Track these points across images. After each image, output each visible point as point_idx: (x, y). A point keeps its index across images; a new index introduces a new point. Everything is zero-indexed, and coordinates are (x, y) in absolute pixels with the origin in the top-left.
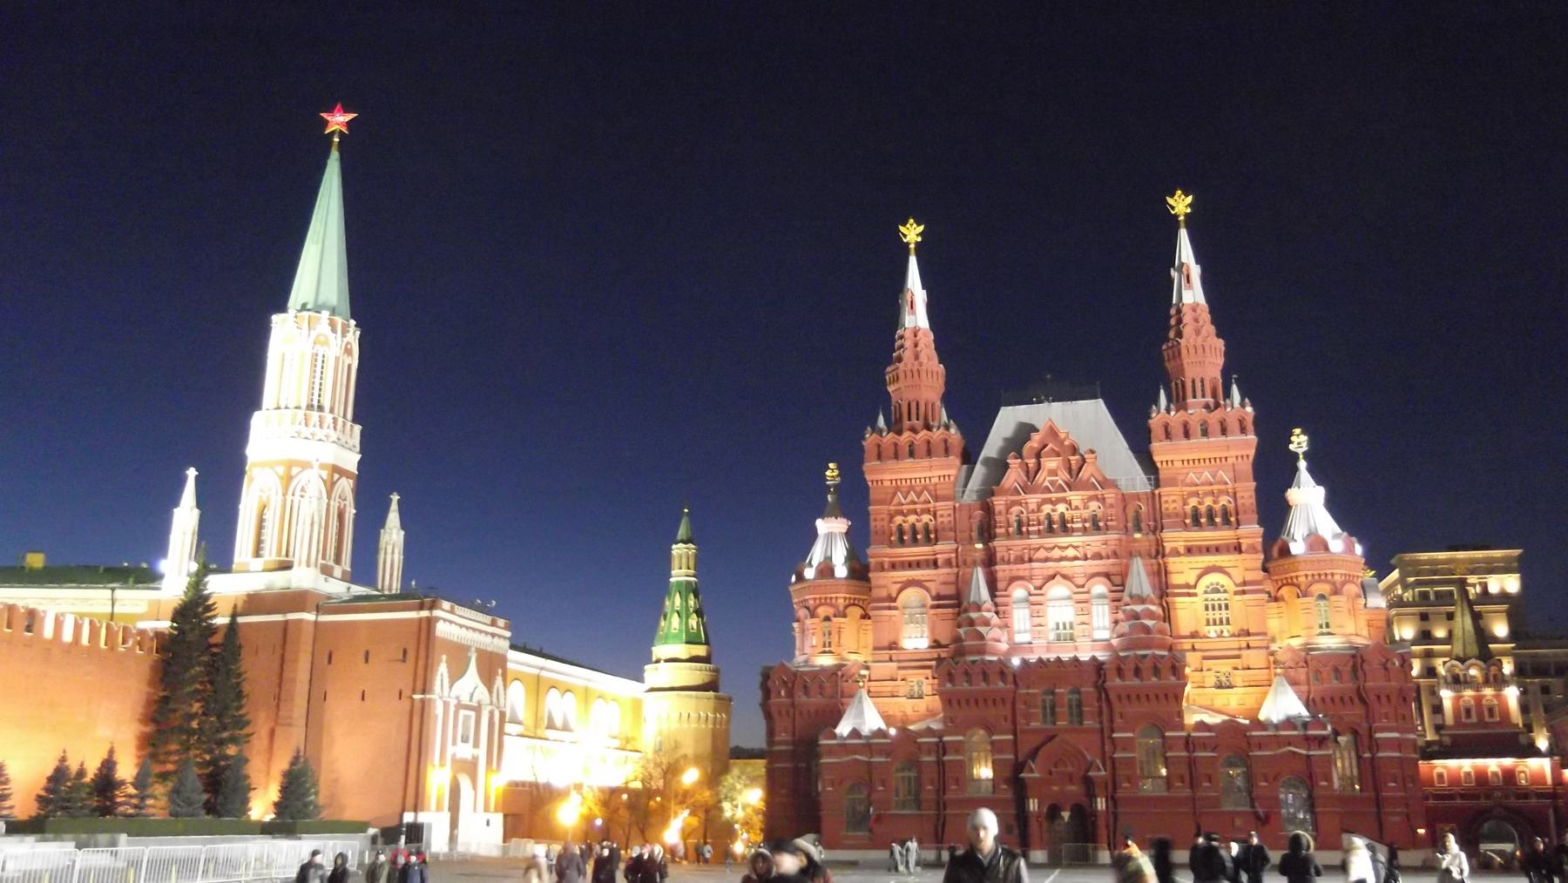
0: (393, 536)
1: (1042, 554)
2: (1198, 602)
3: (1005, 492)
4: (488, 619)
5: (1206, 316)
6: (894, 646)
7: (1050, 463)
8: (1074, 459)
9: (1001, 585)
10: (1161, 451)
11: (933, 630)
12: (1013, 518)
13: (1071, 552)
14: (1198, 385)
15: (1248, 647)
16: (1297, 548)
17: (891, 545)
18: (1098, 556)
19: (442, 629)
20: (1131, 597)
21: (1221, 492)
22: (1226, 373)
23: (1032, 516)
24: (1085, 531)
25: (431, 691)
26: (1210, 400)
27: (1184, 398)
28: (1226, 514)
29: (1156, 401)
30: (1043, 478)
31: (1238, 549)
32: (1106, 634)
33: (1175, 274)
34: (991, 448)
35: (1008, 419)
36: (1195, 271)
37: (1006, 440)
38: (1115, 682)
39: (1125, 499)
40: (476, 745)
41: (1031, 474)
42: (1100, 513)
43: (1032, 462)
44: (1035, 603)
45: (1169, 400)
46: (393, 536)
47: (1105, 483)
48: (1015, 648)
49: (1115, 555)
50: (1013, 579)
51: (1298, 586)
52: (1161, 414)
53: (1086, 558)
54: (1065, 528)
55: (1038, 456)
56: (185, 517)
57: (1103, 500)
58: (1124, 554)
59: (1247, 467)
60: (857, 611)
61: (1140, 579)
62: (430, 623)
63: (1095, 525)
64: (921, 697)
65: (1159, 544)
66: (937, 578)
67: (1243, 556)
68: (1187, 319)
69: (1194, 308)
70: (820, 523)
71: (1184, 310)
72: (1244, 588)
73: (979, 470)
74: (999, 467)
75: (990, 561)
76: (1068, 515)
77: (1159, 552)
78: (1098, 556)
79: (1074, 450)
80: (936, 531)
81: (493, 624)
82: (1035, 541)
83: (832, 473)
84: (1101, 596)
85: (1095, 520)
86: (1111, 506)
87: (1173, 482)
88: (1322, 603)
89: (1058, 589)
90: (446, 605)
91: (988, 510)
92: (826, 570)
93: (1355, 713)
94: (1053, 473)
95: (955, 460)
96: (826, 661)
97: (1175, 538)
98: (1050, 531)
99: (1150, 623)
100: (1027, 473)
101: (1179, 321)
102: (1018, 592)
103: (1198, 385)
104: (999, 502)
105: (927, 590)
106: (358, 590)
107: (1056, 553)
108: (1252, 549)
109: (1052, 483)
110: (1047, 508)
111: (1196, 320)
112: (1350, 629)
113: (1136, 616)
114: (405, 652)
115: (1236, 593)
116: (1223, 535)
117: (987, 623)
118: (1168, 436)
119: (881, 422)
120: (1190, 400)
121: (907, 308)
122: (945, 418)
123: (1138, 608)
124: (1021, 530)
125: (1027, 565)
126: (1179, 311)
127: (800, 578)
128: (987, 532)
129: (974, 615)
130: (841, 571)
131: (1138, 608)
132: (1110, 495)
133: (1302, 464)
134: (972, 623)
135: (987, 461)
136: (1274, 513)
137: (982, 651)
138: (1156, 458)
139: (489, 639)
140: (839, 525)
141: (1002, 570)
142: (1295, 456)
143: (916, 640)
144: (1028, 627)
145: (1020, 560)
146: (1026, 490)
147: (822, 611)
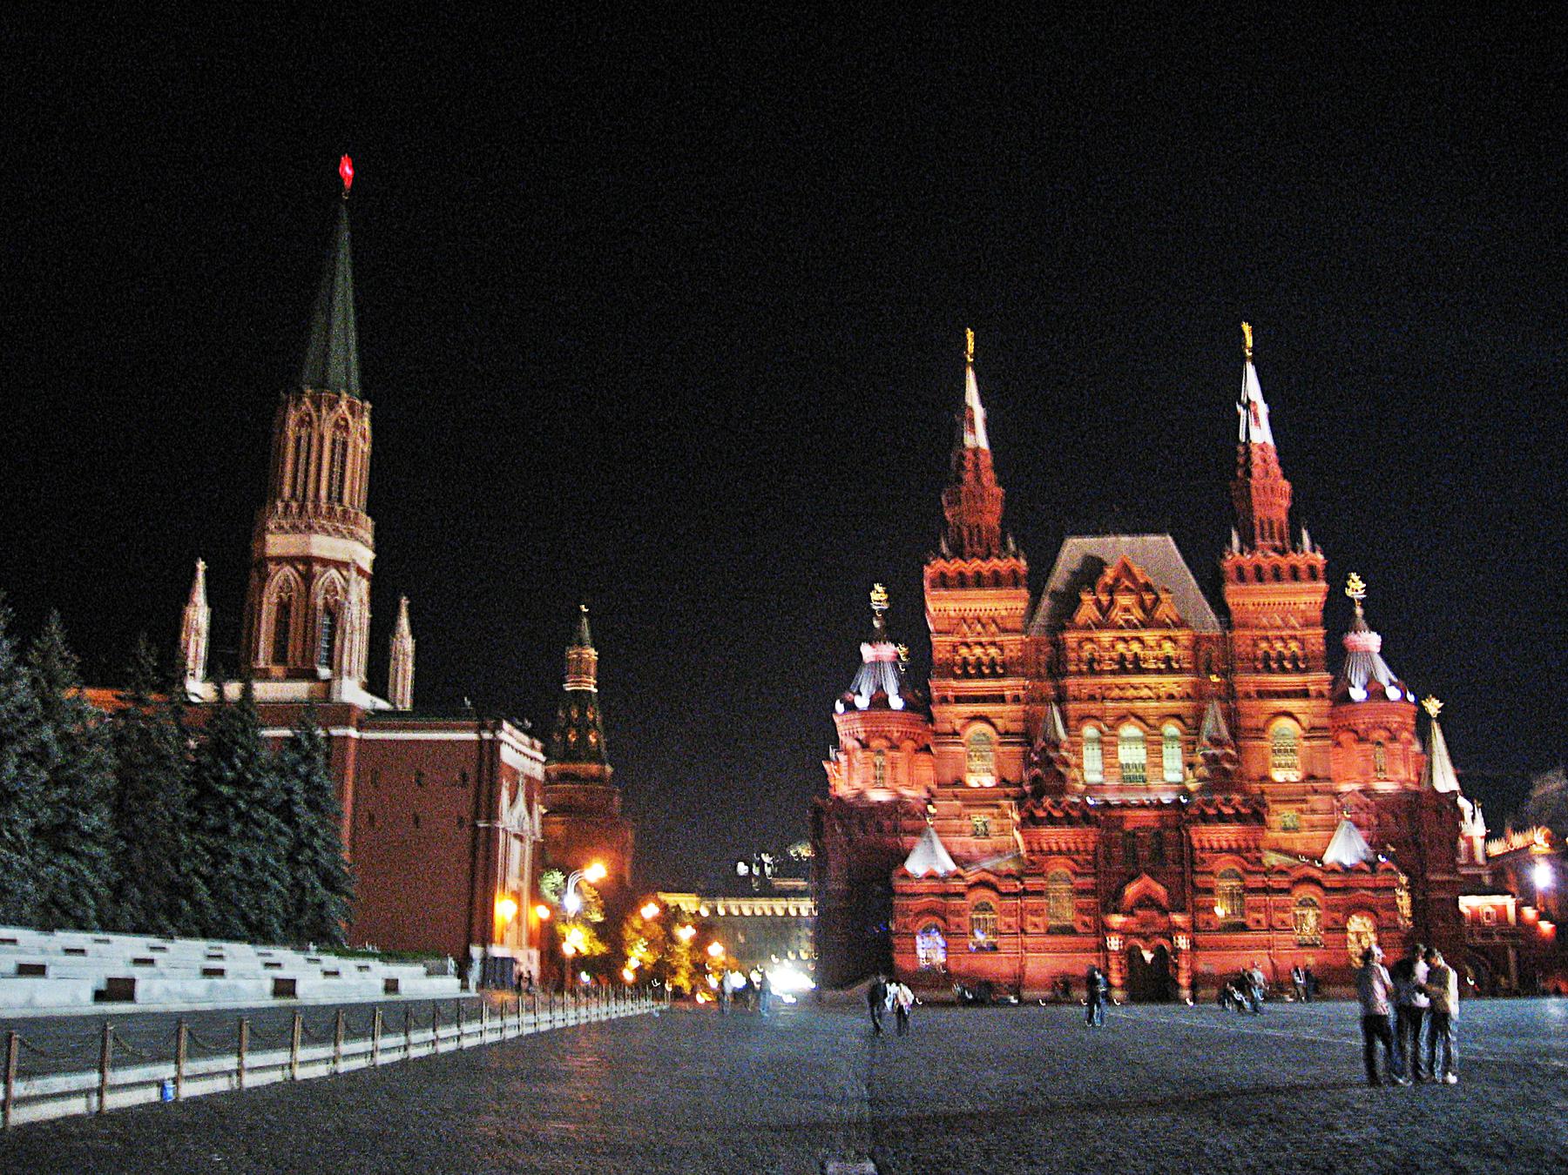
0: (405, 642)
1: (1116, 693)
3: (1076, 628)
4: (526, 739)
5: (1272, 456)
6: (959, 782)
8: (1148, 598)
9: (1072, 723)
10: (1234, 594)
11: (999, 766)
12: (1086, 655)
13: (1145, 692)
14: (1266, 526)
15: (1316, 792)
16: (1358, 694)
17: (956, 677)
18: (1171, 697)
19: (507, 755)
20: (1210, 739)
21: (1294, 638)
22: (1292, 513)
23: (1106, 655)
24: (1158, 672)
25: (497, 818)
26: (1278, 543)
27: (1253, 538)
28: (1294, 659)
29: (1230, 543)
30: (1117, 615)
31: (1304, 694)
32: (1178, 777)
33: (1240, 408)
34: (1059, 578)
35: (1075, 549)
36: (1263, 409)
37: (1074, 573)
40: (521, 877)
41: (1105, 611)
42: (1172, 653)
44: (1107, 745)
45: (1241, 540)
46: (405, 642)
48: (1091, 789)
49: (1189, 696)
50: (1084, 718)
51: (1356, 732)
52: (1235, 554)
53: (1159, 698)
55: (1111, 590)
56: (199, 614)
57: (1173, 640)
58: (1198, 695)
59: (1316, 614)
60: (909, 745)
61: (1214, 721)
62: (495, 745)
63: (1168, 667)
64: (987, 835)
65: (1230, 686)
66: (1006, 714)
67: (1314, 703)
68: (1256, 458)
69: (1263, 447)
70: (867, 652)
71: (1255, 450)
72: (1312, 732)
73: (1046, 602)
74: (1068, 603)
75: (1061, 699)
76: (1141, 654)
77: (1229, 694)
78: (1171, 697)
79: (1148, 587)
80: (1003, 666)
81: (532, 746)
82: (1108, 680)
83: (878, 596)
84: (1173, 738)
85: (1167, 660)
86: (1186, 648)
87: (1245, 626)
88: (1379, 750)
89: (1130, 730)
90: (506, 726)
91: (1058, 646)
92: (879, 701)
93: (1409, 856)
94: (1126, 610)
95: (1024, 592)
96: (879, 796)
98: (1123, 671)
99: (1228, 766)
100: (1100, 608)
101: (1248, 459)
102: (1089, 731)
103: (1266, 526)
104: (1071, 638)
105: (993, 725)
106: (382, 705)
107: (1131, 693)
108: (1320, 695)
109: (1126, 621)
110: (1121, 647)
111: (1265, 461)
112: (1403, 775)
114: (464, 777)
115: (1306, 738)
116: (1294, 680)
117: (1066, 764)
118: (1241, 577)
119: (945, 549)
120: (1259, 542)
121: (966, 426)
122: (1012, 546)
123: (1217, 752)
124: (1093, 667)
125: (1099, 705)
126: (1248, 451)
127: (850, 707)
128: (1057, 668)
129: (1052, 754)
130: (896, 703)
131: (1217, 752)
132: (1183, 636)
133: (1359, 611)
134: (1050, 761)
135: (1055, 594)
136: (1337, 657)
138: (1230, 601)
139: (527, 762)
140: (887, 651)
141: (1072, 707)
142: (1352, 600)
143: (981, 778)
144: (1100, 767)
145: (1092, 698)
146: (1100, 626)
147: (874, 744)
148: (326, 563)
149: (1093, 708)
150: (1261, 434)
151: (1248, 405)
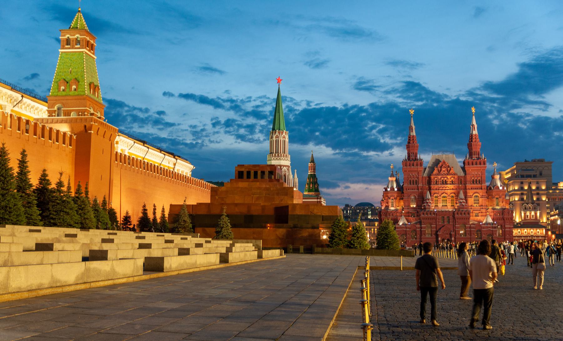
2: (473, 199)
7: (444, 169)
18: (453, 189)
24: (450, 184)
31: (481, 189)
38: (456, 216)
39: (459, 177)
43: (440, 169)
47: (455, 174)
54: (446, 183)
55: (441, 167)
60: (398, 198)
63: (452, 183)
65: (466, 187)
68: (474, 137)
75: (430, 189)
77: (465, 188)
78: (453, 189)
79: (449, 167)
82: (440, 186)
85: (452, 181)
91: (429, 177)
92: (392, 189)
97: (469, 186)
98: (443, 183)
104: (432, 177)
113: (461, 202)
130: (396, 189)
132: (456, 177)
134: (427, 203)
137: (429, 209)
145: (436, 189)
148: (284, 166)
149: (437, 191)
150: (475, 132)
151: (473, 125)
